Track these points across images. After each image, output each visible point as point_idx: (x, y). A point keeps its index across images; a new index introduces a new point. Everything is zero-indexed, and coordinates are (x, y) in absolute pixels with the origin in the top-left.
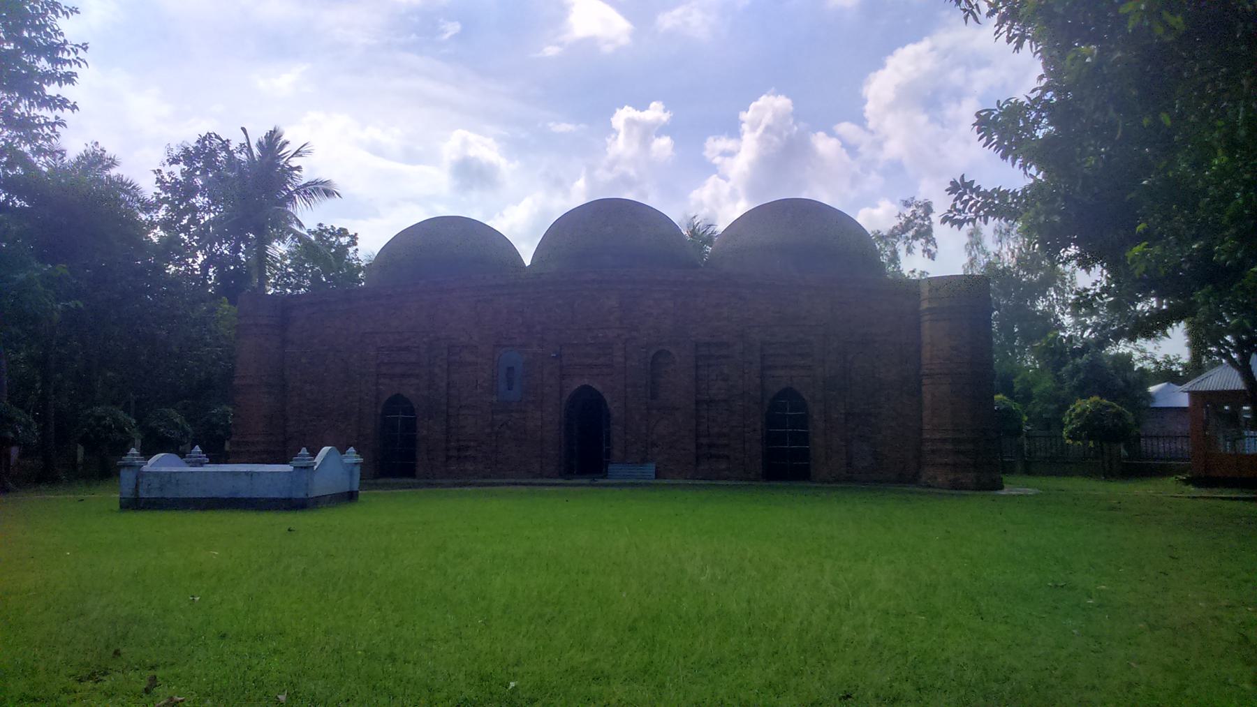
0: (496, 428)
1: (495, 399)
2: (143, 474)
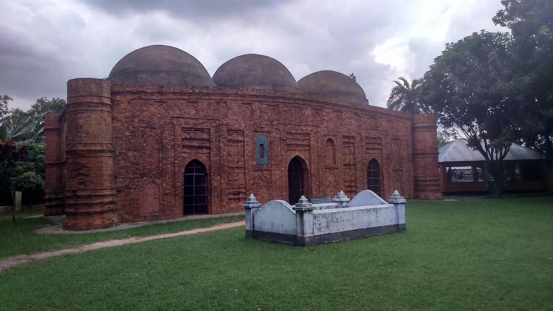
1: (254, 163)
2: (315, 217)
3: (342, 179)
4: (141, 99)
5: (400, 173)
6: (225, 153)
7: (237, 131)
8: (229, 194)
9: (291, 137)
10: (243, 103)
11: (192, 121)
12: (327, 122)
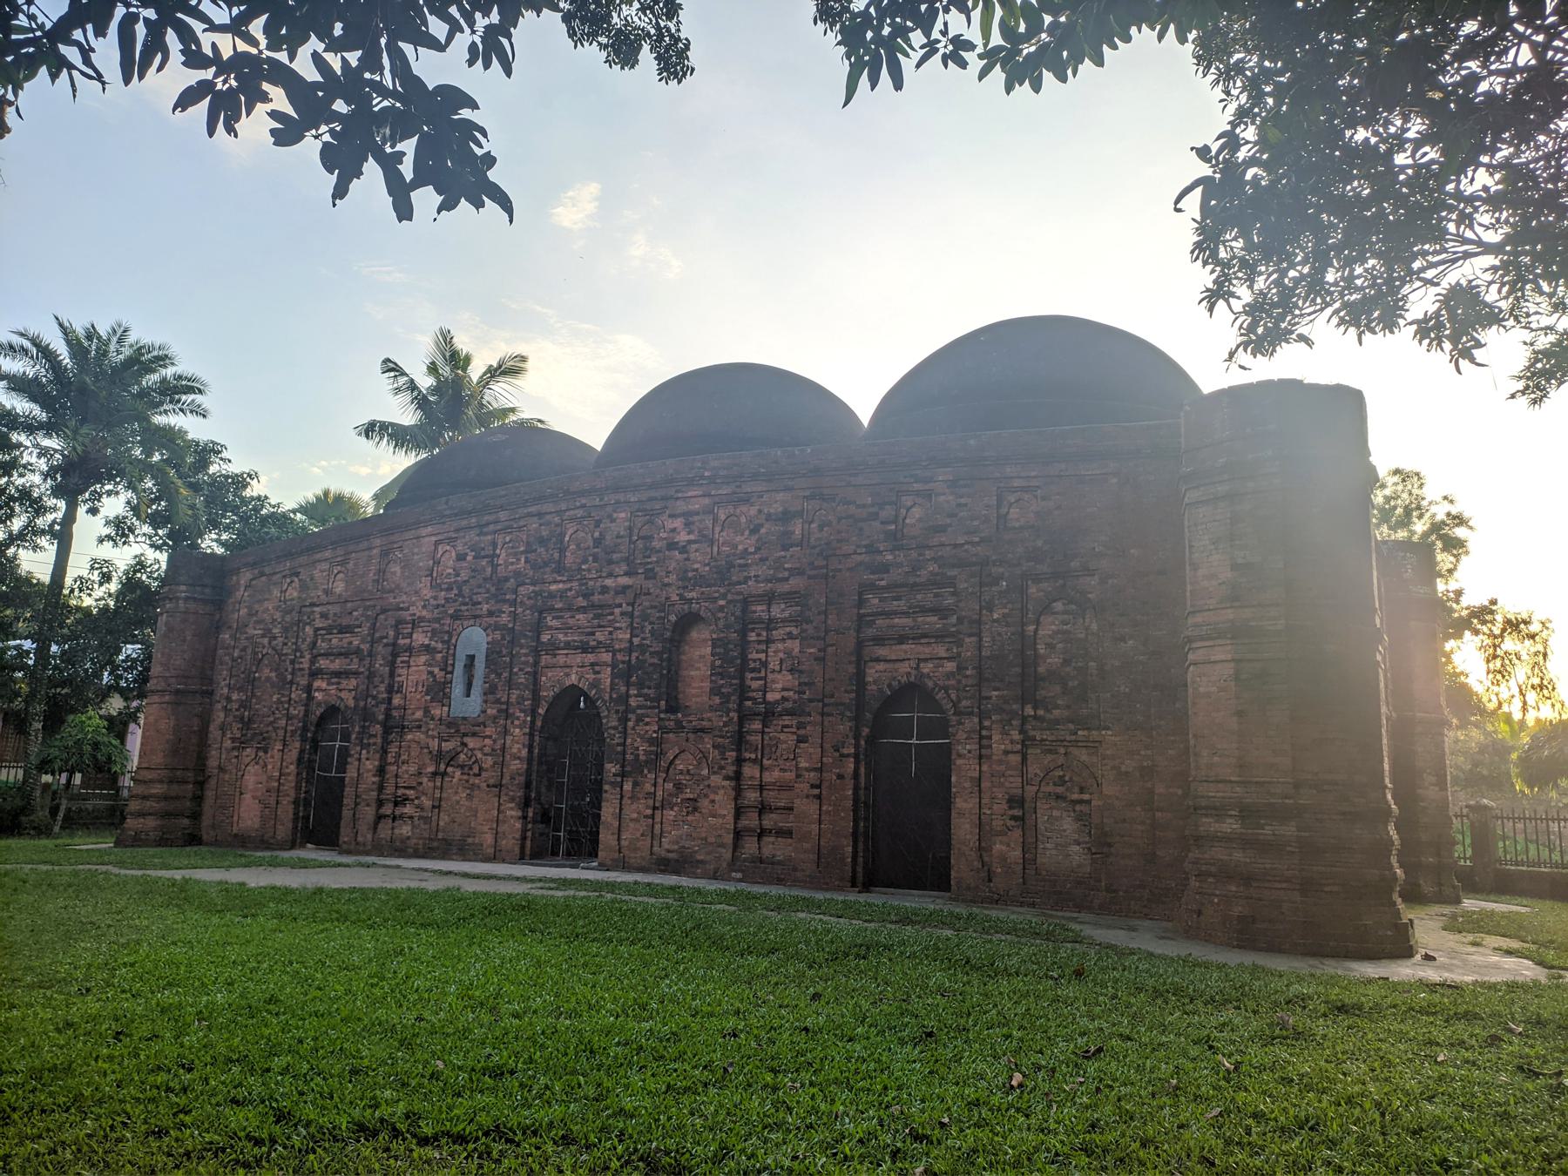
0: (442, 766)
3: (727, 778)
4: (262, 574)
5: (1084, 756)
6: (382, 688)
7: (415, 624)
8: (380, 803)
9: (555, 623)
10: (437, 543)
11: (334, 609)
12: (684, 550)
